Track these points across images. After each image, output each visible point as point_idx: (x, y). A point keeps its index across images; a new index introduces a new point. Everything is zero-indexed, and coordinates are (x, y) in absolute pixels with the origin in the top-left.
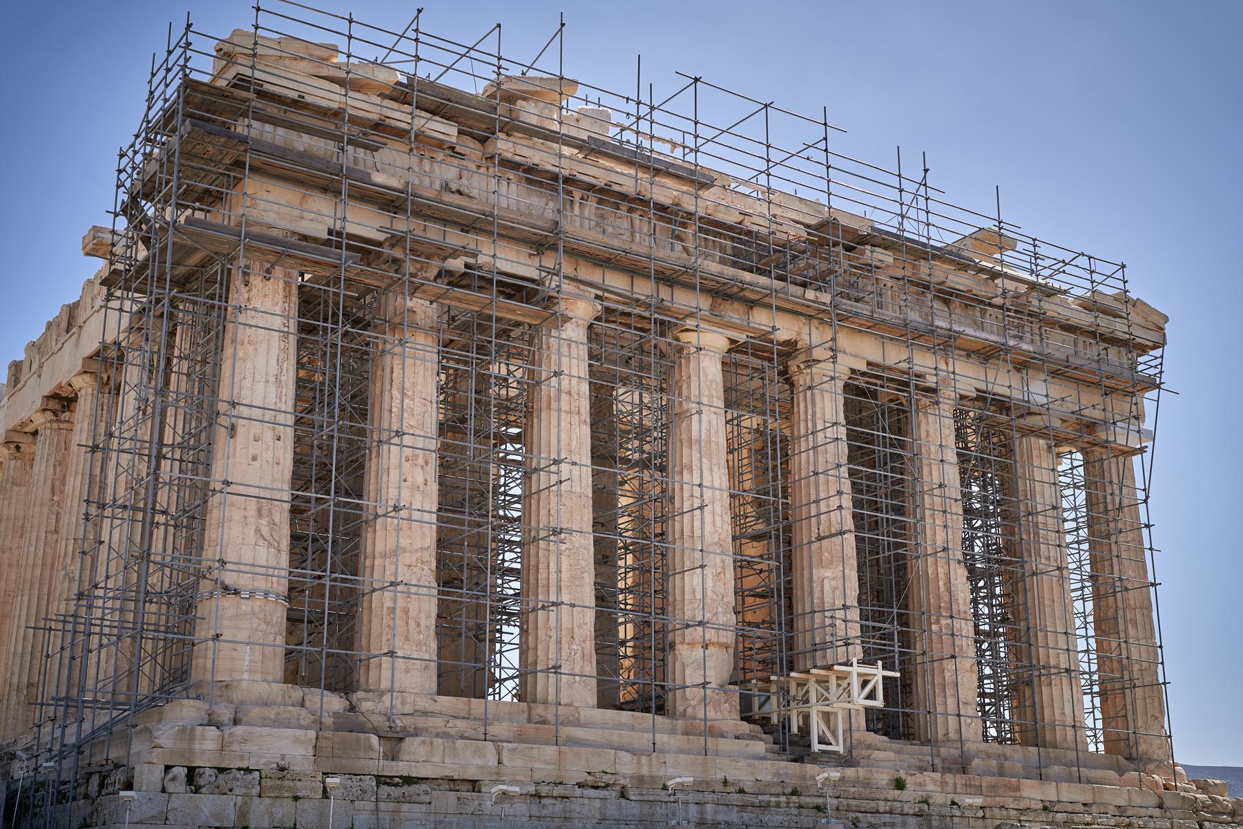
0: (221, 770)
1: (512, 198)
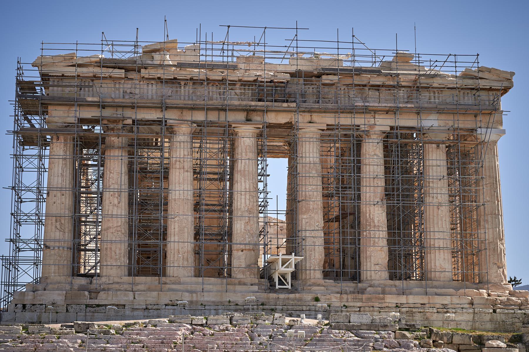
0: (33, 305)
1: (152, 91)
